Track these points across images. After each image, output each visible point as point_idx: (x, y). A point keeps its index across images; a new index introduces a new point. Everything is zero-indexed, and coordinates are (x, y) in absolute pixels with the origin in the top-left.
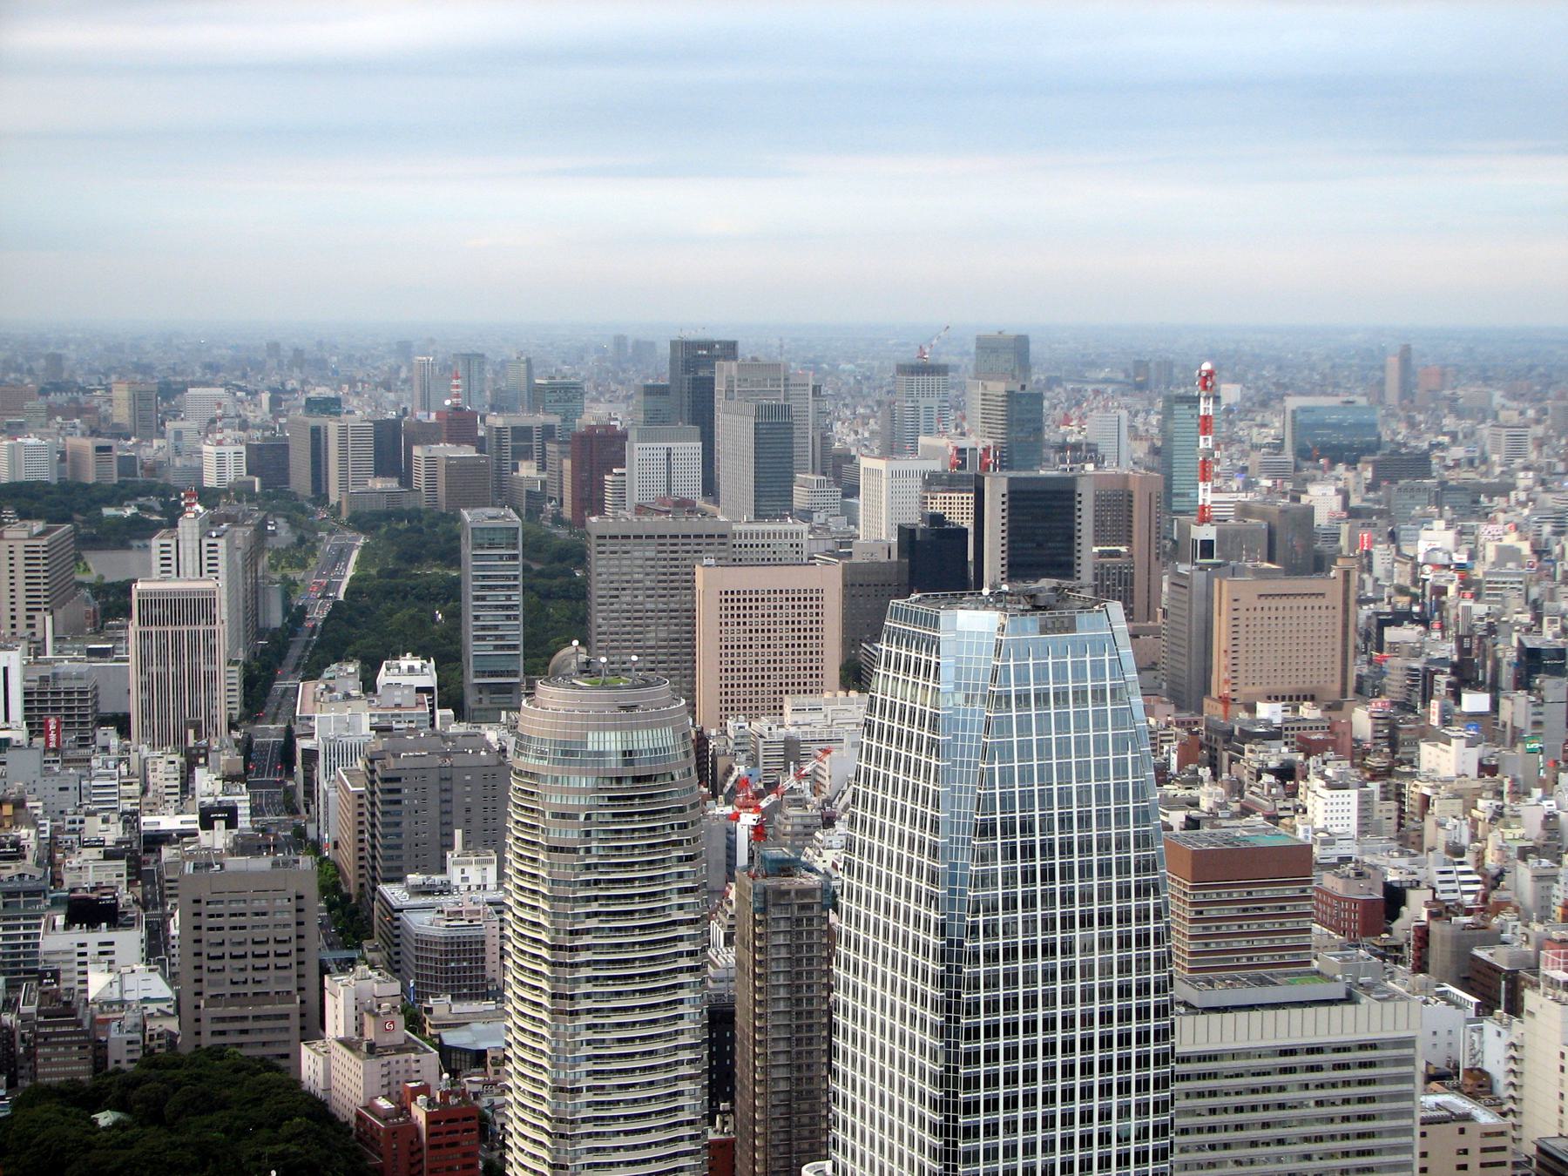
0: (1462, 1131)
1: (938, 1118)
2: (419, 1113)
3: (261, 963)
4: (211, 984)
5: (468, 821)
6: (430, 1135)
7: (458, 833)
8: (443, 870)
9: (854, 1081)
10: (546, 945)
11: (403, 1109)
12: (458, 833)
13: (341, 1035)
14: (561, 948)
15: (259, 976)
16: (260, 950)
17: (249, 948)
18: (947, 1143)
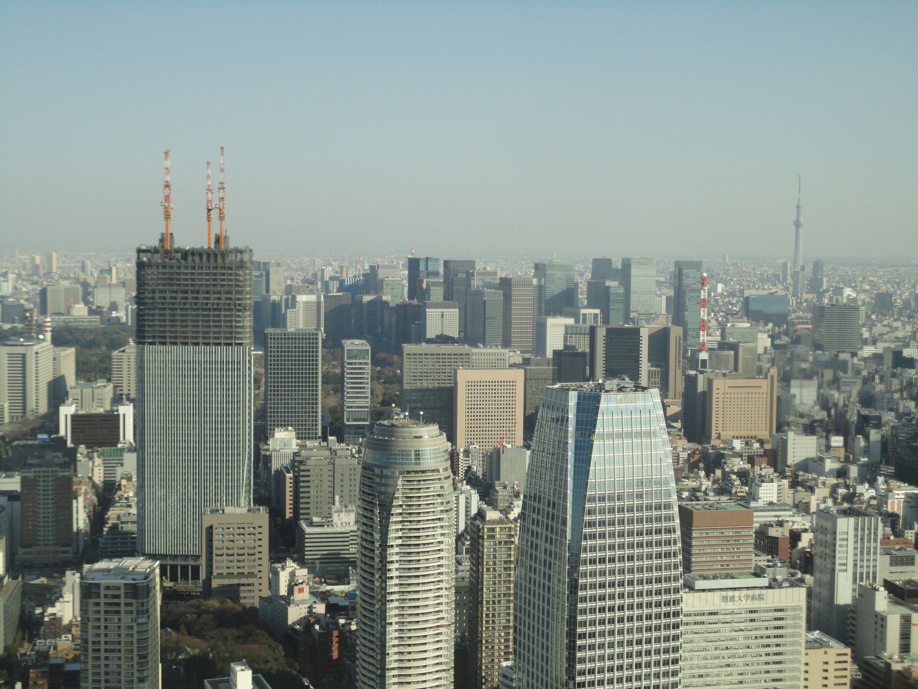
3: (241, 558)
5: (342, 491)
7: (337, 498)
8: (330, 515)
15: (240, 564)
16: (241, 552)
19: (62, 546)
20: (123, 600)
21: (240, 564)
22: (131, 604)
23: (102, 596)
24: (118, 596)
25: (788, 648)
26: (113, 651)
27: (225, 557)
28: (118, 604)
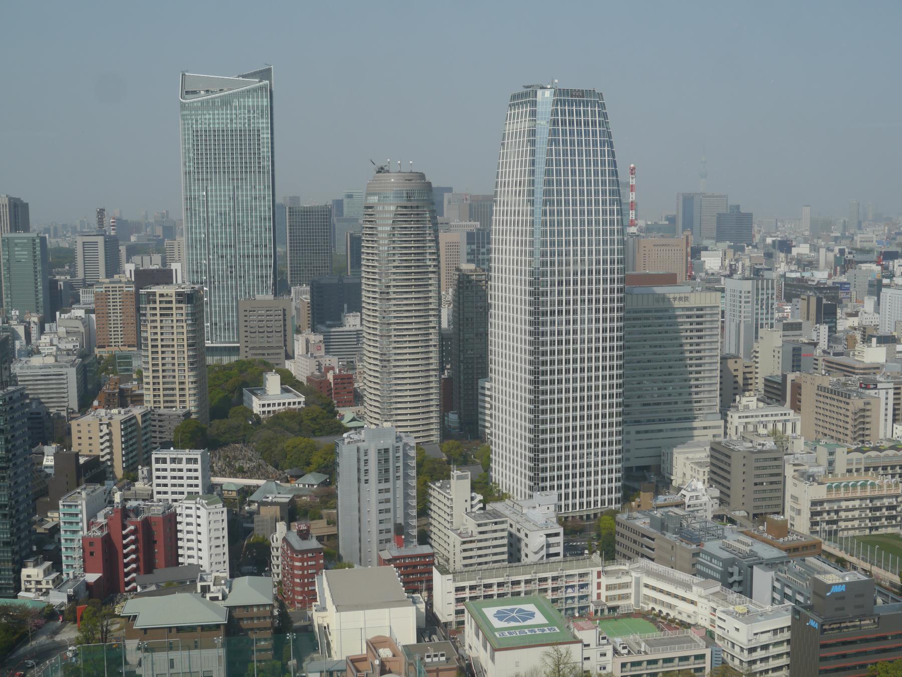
0: (736, 362)
1: (532, 474)
2: (330, 376)
3: (270, 335)
4: (251, 342)
6: (335, 384)
7: (346, 306)
10: (379, 335)
12: (346, 306)
14: (384, 293)
15: (269, 340)
17: (266, 329)
18: (535, 387)
19: (129, 346)
20: (174, 305)
21: (269, 340)
22: (182, 308)
24: (171, 302)
25: (707, 354)
26: (168, 346)
27: (257, 334)
28: (171, 308)
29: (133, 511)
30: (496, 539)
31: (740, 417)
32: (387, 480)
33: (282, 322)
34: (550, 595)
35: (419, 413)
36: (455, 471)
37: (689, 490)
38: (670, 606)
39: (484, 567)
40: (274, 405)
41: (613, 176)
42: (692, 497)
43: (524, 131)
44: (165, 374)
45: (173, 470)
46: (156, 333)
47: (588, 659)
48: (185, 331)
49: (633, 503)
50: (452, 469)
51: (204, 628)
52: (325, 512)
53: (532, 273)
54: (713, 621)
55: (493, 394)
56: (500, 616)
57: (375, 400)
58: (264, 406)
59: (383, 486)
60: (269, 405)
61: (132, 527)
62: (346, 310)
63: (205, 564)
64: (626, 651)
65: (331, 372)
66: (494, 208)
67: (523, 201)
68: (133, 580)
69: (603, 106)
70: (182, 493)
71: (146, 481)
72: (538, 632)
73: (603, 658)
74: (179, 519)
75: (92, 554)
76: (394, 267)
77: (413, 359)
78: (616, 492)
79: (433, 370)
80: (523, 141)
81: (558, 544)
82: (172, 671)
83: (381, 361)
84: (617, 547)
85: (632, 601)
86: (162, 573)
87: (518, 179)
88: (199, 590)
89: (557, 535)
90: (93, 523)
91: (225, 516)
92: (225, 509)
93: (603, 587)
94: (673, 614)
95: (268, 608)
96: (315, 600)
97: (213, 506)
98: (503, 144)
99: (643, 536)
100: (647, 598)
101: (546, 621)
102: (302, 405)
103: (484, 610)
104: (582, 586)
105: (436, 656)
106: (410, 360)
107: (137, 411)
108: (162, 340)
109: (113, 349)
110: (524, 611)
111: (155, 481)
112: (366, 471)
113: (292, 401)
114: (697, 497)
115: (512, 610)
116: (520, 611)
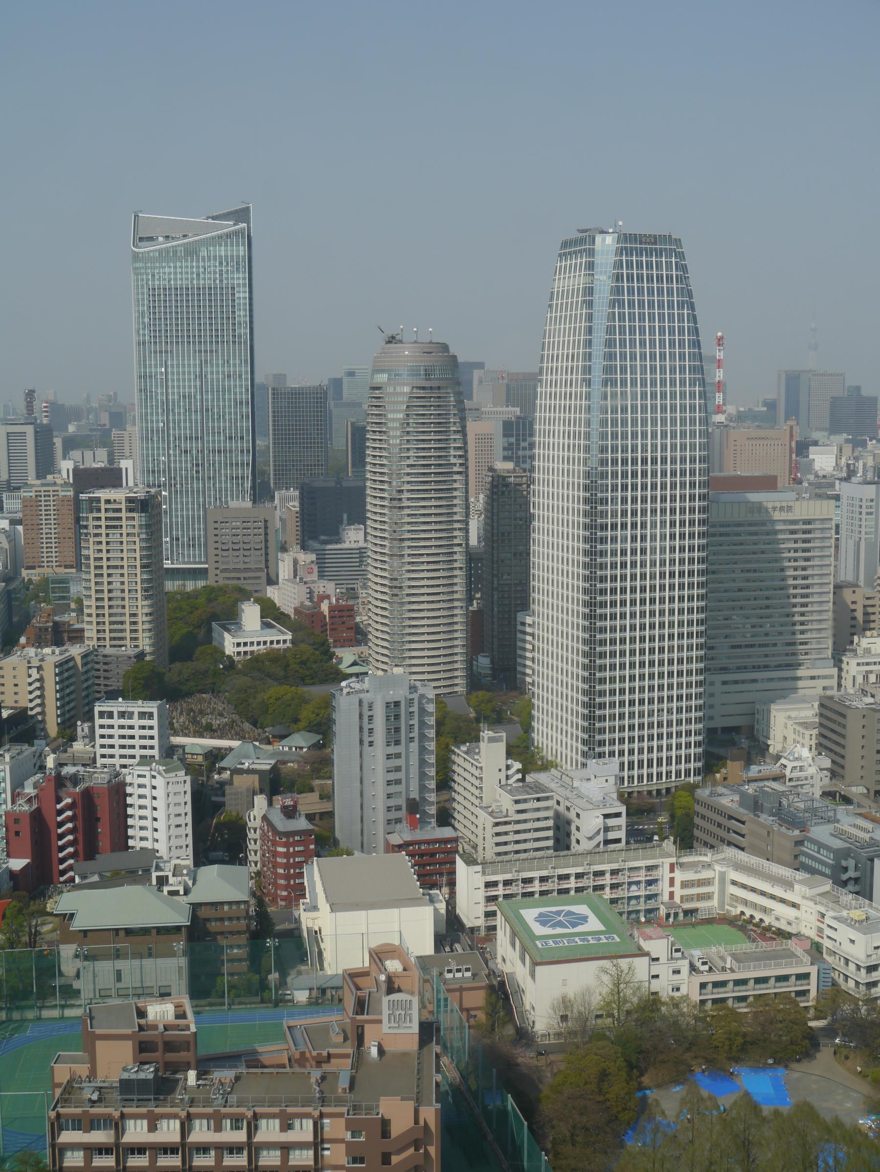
0: (854, 592)
1: (586, 736)
2: (325, 607)
3: (246, 553)
4: (223, 563)
6: (331, 617)
7: (345, 517)
9: (543, 709)
10: (388, 555)
11: (317, 605)
12: (345, 517)
13: (287, 578)
14: (395, 499)
17: (242, 545)
18: (591, 623)
19: (66, 567)
20: (123, 514)
23: (103, 510)
24: (119, 510)
26: (116, 567)
28: (120, 519)
29: (70, 779)
30: (538, 819)
31: (858, 664)
32: (397, 743)
33: (262, 537)
34: (607, 894)
35: (440, 656)
36: (486, 732)
37: (791, 758)
38: (765, 910)
39: (523, 856)
40: (252, 643)
41: (694, 347)
42: (794, 768)
43: (578, 289)
44: (111, 603)
45: (122, 727)
46: (100, 551)
47: (657, 976)
48: (137, 547)
49: (718, 775)
50: (482, 729)
51: (161, 931)
52: (316, 783)
53: (588, 475)
54: (820, 930)
55: (536, 632)
56: (543, 920)
57: (382, 639)
58: (239, 645)
59: (393, 750)
60: (245, 644)
61: (69, 800)
62: (345, 522)
63: (162, 848)
64: (706, 968)
65: (326, 602)
66: (539, 390)
67: (577, 380)
68: (70, 868)
69: (681, 256)
70: (133, 757)
71: (87, 740)
72: (592, 942)
73: (676, 976)
74: (129, 790)
75: (17, 833)
76: (408, 466)
77: (432, 586)
78: (695, 761)
79: (458, 600)
80: (577, 302)
81: (619, 828)
82: (119, 985)
83: (391, 587)
84: (696, 833)
85: (715, 902)
86: (106, 859)
87: (571, 351)
88: (154, 882)
89: (618, 815)
90: (19, 794)
91: (188, 787)
92: (188, 778)
93: (677, 883)
94: (768, 920)
95: (242, 907)
96: (303, 896)
97: (173, 774)
98: (550, 306)
99: (731, 818)
100: (735, 899)
101: (603, 928)
102: (288, 644)
103: (522, 912)
104: (650, 883)
105: (459, 971)
106: (428, 586)
107: (76, 651)
108: (108, 559)
109: (47, 571)
110: (574, 914)
111: (99, 741)
112: (371, 731)
113: (275, 638)
114: (801, 768)
115: (558, 913)
116: (569, 913)
